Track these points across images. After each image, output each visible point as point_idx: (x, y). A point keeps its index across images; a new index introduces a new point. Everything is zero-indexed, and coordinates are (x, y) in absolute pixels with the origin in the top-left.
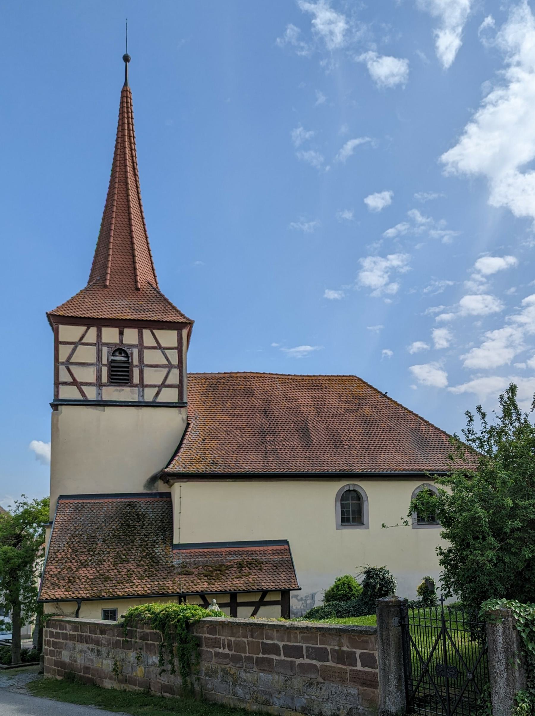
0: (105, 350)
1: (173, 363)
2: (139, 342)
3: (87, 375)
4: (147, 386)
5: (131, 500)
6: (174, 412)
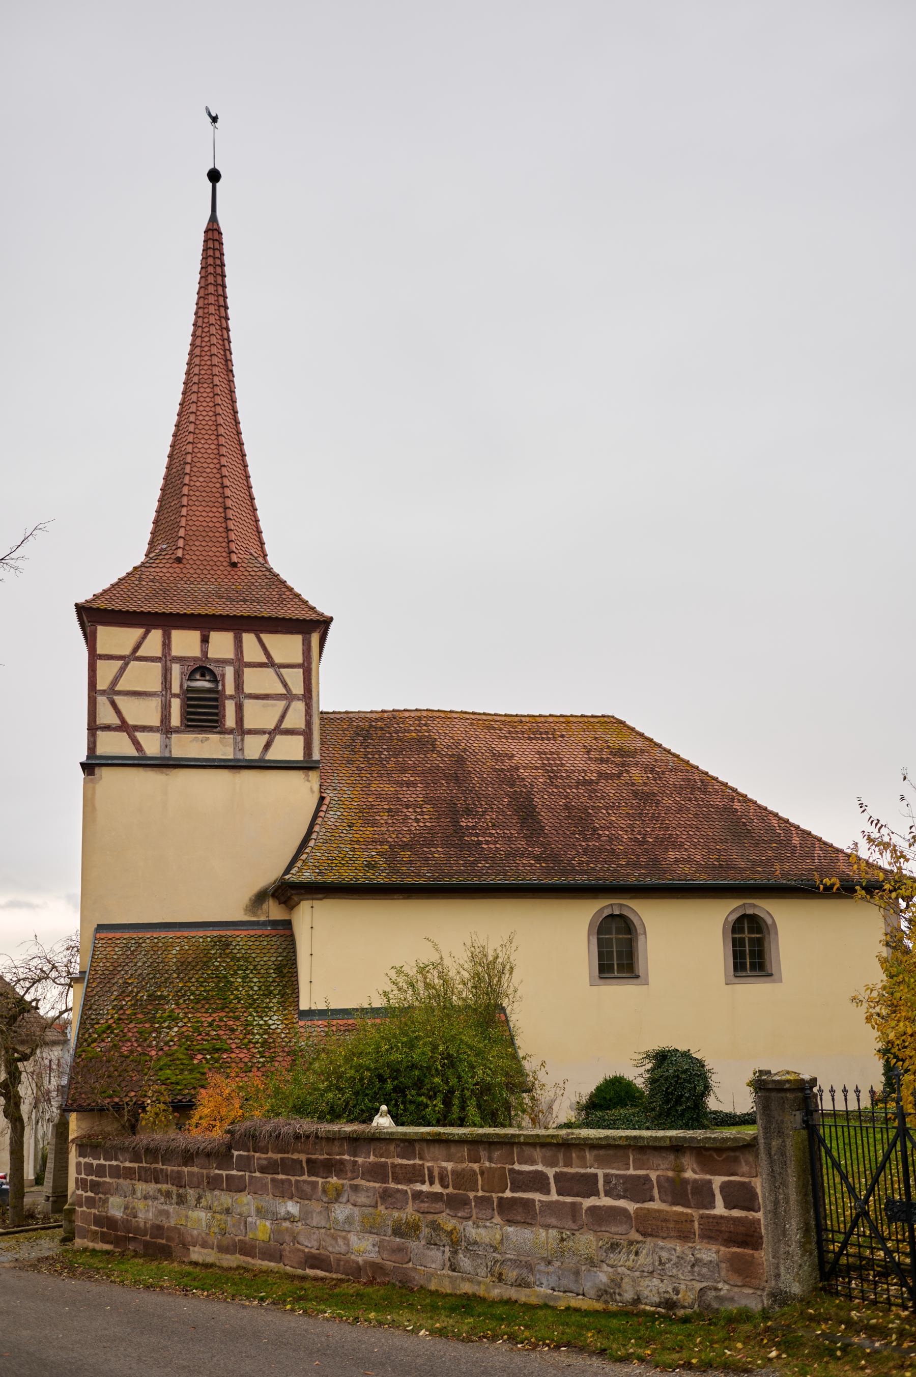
0: (176, 669)
1: (295, 692)
2: (236, 655)
3: (144, 712)
4: (251, 732)
5: (222, 933)
6: (295, 778)
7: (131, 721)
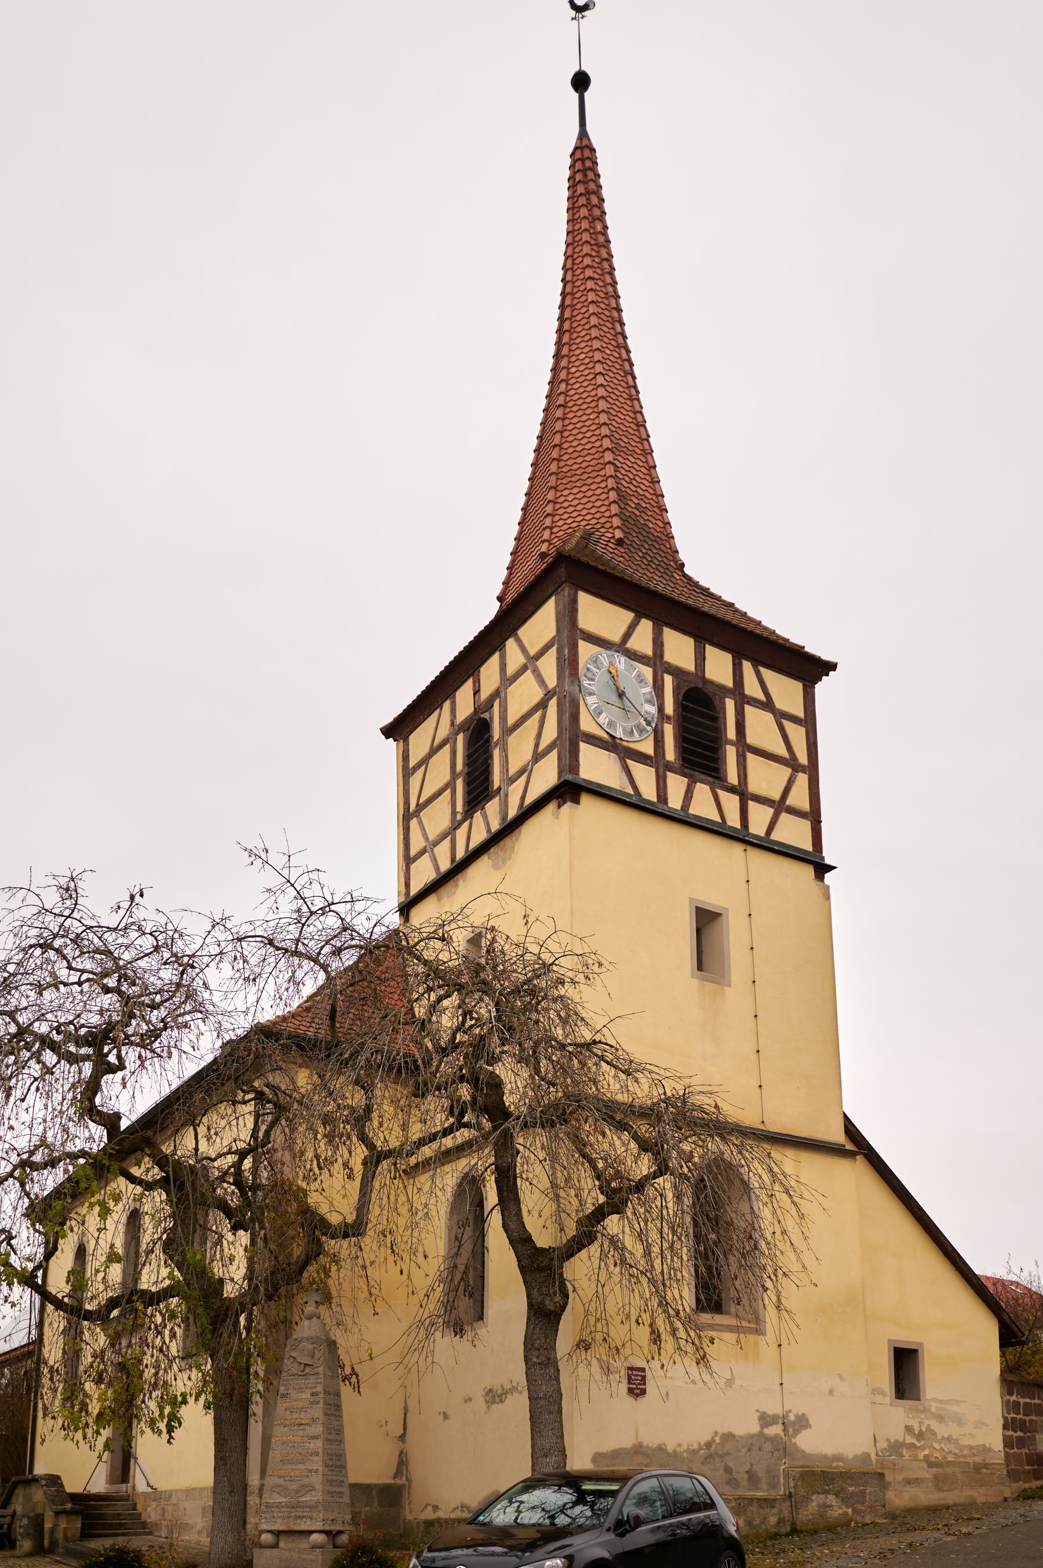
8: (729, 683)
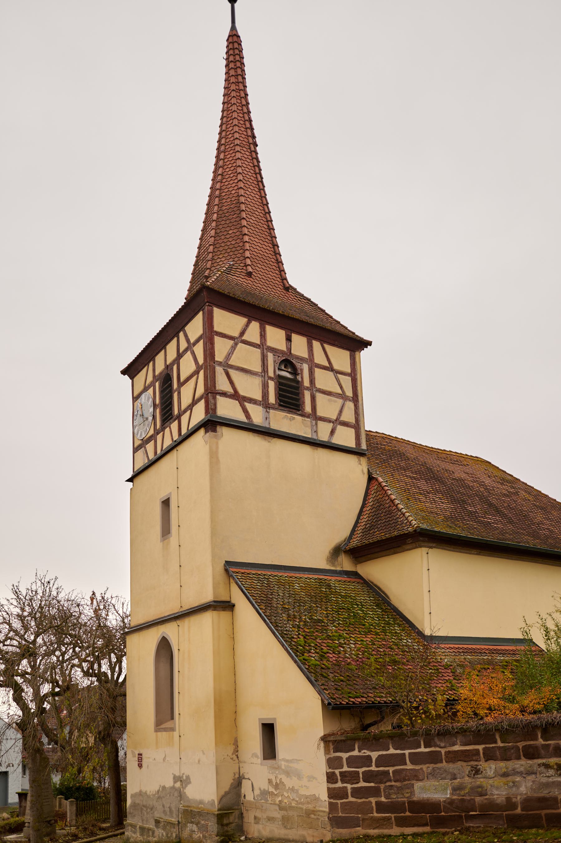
0: (270, 357)
2: (309, 356)
3: (250, 387)
7: (242, 393)
8: (305, 355)
